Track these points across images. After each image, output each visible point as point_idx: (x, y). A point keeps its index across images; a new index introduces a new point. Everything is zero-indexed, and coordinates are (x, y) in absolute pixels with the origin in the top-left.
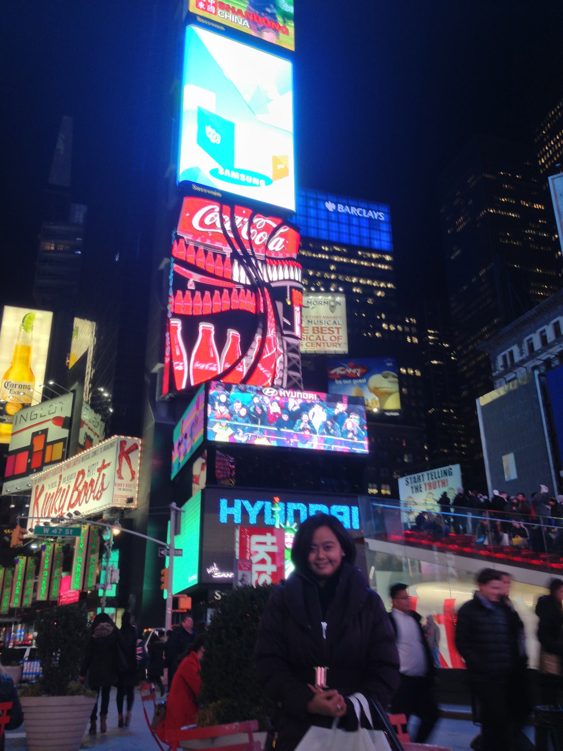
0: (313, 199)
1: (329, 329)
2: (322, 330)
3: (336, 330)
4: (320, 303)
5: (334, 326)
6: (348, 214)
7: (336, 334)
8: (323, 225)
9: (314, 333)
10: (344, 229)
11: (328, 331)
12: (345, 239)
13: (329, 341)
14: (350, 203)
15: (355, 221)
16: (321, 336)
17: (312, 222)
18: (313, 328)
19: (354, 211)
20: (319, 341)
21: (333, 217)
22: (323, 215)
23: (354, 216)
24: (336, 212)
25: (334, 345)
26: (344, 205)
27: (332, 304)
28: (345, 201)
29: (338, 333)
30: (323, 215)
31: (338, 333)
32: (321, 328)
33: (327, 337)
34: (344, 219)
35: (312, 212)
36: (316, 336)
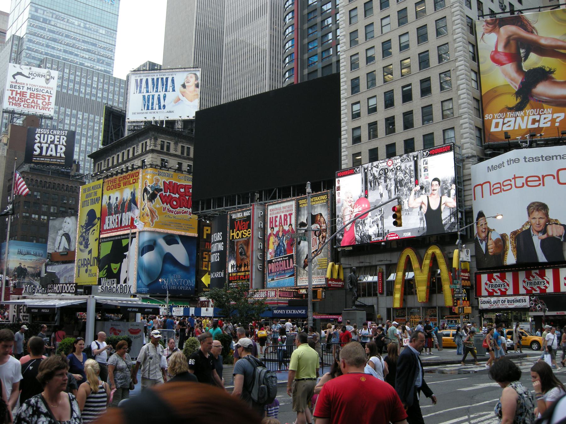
1: (42, 96)
2: (37, 97)
3: (47, 98)
5: (47, 94)
7: (47, 101)
9: (30, 97)
11: (41, 98)
13: (41, 105)
16: (35, 100)
18: (31, 93)
20: (33, 104)
25: (43, 108)
27: (48, 77)
29: (49, 100)
31: (49, 100)
32: (37, 94)
33: (40, 102)
36: (32, 99)
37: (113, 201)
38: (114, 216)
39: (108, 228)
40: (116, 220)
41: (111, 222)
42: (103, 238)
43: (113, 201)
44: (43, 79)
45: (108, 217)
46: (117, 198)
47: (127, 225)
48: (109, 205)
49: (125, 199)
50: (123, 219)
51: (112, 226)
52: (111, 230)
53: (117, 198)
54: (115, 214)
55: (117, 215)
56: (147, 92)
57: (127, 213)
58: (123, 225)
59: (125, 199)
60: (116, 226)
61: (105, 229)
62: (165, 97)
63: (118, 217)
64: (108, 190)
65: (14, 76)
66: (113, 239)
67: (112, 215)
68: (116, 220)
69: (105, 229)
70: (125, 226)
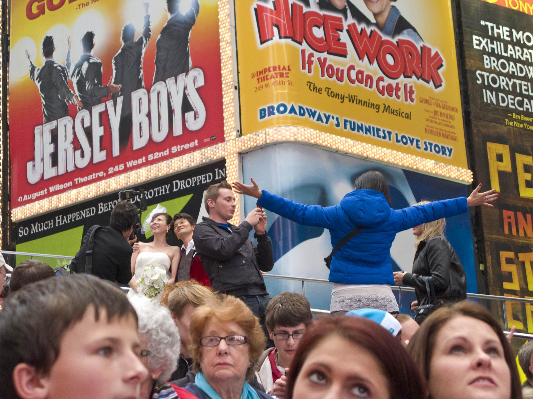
37: (69, 54)
38: (83, 114)
39: (50, 173)
40: (98, 132)
41: (65, 144)
42: (27, 222)
43: (69, 54)
45: (48, 127)
46: (89, 40)
47: (159, 137)
48: (51, 77)
49: (139, 32)
50: (138, 118)
51: (70, 160)
52: (71, 178)
53: (89, 40)
54: (87, 105)
55: (97, 109)
57: (159, 86)
58: (138, 142)
59: (139, 32)
60: (100, 156)
61: (33, 178)
63: (104, 118)
64: (31, 16)
66: (86, 214)
67: (69, 111)
68: (98, 132)
69: (33, 178)
70: (152, 146)
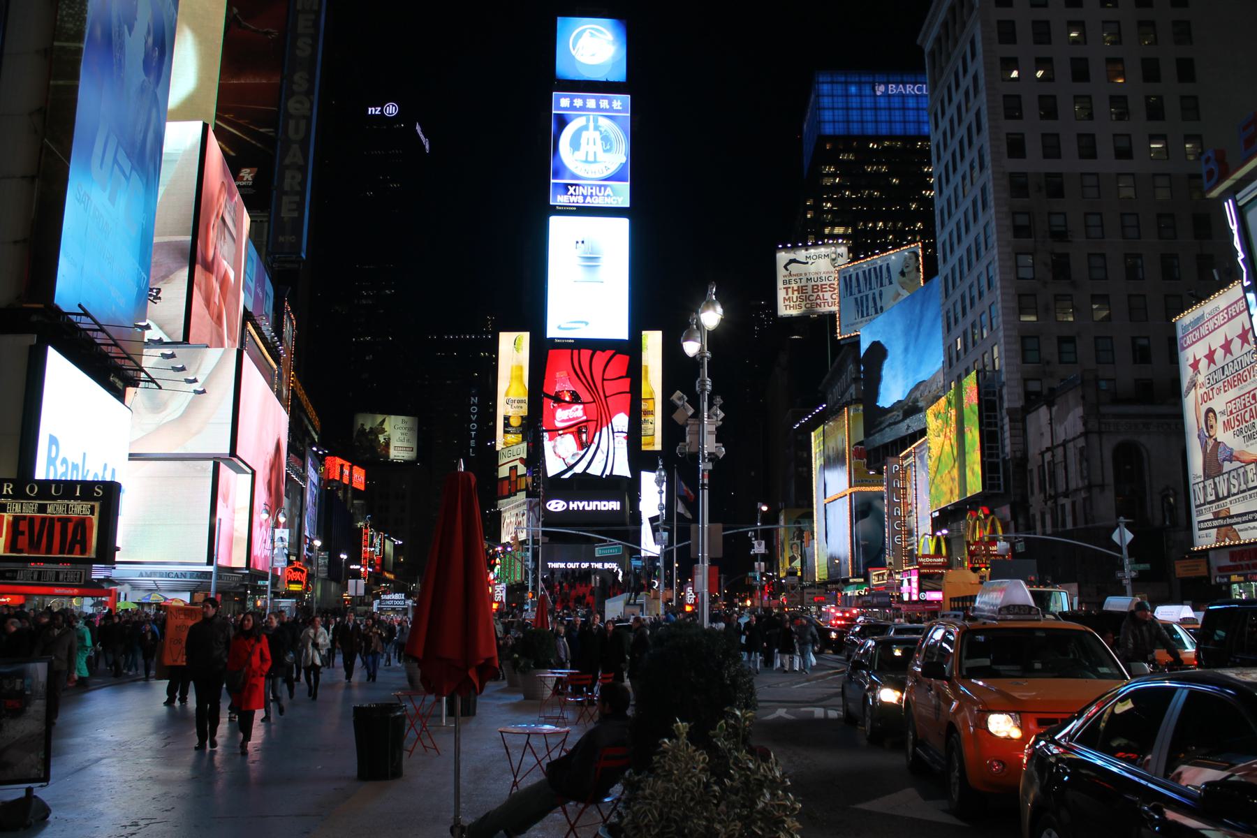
0: (855, 83)
4: (819, 257)
6: (903, 96)
8: (869, 115)
10: (897, 115)
12: (898, 129)
13: (830, 300)
14: (905, 79)
15: (911, 103)
17: (855, 115)
19: (910, 89)
21: (883, 103)
22: (868, 102)
23: (910, 96)
24: (886, 95)
26: (897, 83)
28: (899, 79)
30: (868, 102)
33: (827, 295)
34: (897, 103)
35: (854, 102)
44: (828, 260)
56: (860, 292)
62: (881, 295)
65: (785, 267)
